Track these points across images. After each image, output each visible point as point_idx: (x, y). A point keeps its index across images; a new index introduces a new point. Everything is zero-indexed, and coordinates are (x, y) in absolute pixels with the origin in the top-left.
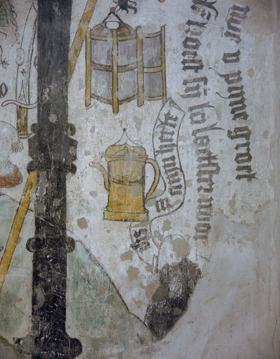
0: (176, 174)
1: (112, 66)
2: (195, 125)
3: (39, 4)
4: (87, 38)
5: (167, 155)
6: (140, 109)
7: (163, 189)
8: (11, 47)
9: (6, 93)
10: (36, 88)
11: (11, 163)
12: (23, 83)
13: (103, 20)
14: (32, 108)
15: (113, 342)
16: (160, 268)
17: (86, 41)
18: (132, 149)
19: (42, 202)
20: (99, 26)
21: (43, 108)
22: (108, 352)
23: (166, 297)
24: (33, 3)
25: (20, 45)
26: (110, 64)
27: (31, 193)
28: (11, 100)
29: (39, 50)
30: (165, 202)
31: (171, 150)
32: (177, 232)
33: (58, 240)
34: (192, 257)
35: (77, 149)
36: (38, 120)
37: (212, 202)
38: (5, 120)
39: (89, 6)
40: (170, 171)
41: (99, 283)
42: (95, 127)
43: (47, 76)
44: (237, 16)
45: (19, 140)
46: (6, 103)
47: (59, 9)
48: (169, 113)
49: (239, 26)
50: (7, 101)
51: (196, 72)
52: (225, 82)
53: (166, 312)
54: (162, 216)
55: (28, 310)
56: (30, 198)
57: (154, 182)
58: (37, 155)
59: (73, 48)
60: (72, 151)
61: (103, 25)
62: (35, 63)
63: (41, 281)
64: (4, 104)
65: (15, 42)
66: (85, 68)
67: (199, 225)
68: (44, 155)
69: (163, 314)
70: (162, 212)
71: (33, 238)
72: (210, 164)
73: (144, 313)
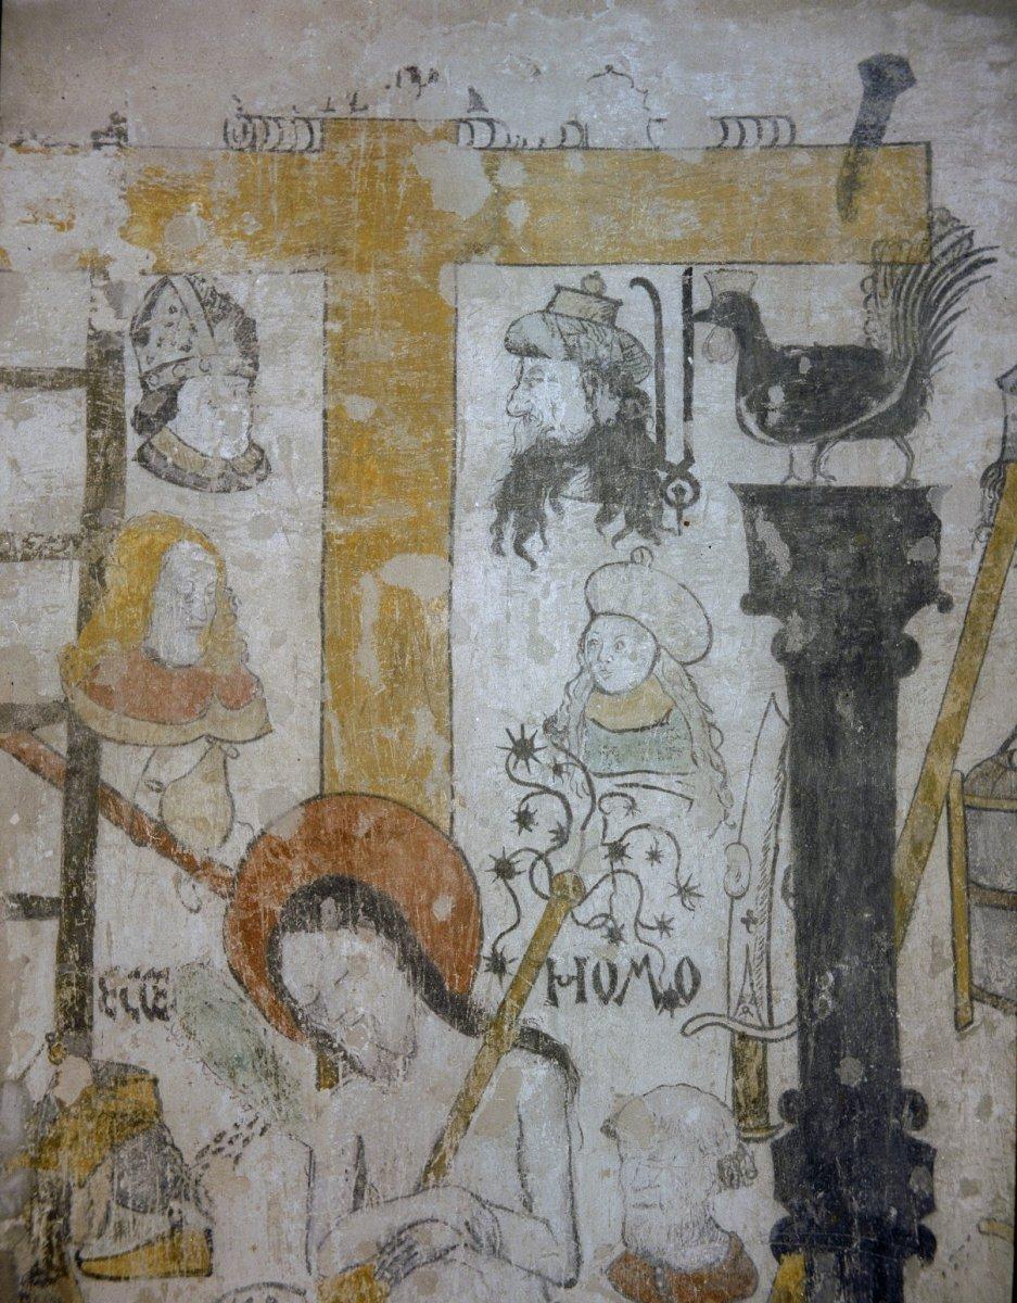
3: (792, 698)
4: (952, 805)
8: (705, 839)
9: (694, 992)
10: (791, 972)
11: (717, 1226)
13: (1000, 743)
14: (782, 1039)
17: (949, 814)
20: (990, 763)
21: (817, 1039)
24: (773, 694)
25: (736, 832)
28: (713, 1015)
29: (796, 844)
35: (937, 1175)
36: (803, 1078)
39: (955, 700)
42: (989, 1097)
43: (827, 932)
45: (740, 1146)
47: (857, 710)
50: (698, 1017)
58: (804, 1196)
59: (907, 838)
60: (918, 1183)
61: (1003, 759)
62: (784, 889)
64: (691, 1027)
66: (948, 903)
68: (825, 1197)
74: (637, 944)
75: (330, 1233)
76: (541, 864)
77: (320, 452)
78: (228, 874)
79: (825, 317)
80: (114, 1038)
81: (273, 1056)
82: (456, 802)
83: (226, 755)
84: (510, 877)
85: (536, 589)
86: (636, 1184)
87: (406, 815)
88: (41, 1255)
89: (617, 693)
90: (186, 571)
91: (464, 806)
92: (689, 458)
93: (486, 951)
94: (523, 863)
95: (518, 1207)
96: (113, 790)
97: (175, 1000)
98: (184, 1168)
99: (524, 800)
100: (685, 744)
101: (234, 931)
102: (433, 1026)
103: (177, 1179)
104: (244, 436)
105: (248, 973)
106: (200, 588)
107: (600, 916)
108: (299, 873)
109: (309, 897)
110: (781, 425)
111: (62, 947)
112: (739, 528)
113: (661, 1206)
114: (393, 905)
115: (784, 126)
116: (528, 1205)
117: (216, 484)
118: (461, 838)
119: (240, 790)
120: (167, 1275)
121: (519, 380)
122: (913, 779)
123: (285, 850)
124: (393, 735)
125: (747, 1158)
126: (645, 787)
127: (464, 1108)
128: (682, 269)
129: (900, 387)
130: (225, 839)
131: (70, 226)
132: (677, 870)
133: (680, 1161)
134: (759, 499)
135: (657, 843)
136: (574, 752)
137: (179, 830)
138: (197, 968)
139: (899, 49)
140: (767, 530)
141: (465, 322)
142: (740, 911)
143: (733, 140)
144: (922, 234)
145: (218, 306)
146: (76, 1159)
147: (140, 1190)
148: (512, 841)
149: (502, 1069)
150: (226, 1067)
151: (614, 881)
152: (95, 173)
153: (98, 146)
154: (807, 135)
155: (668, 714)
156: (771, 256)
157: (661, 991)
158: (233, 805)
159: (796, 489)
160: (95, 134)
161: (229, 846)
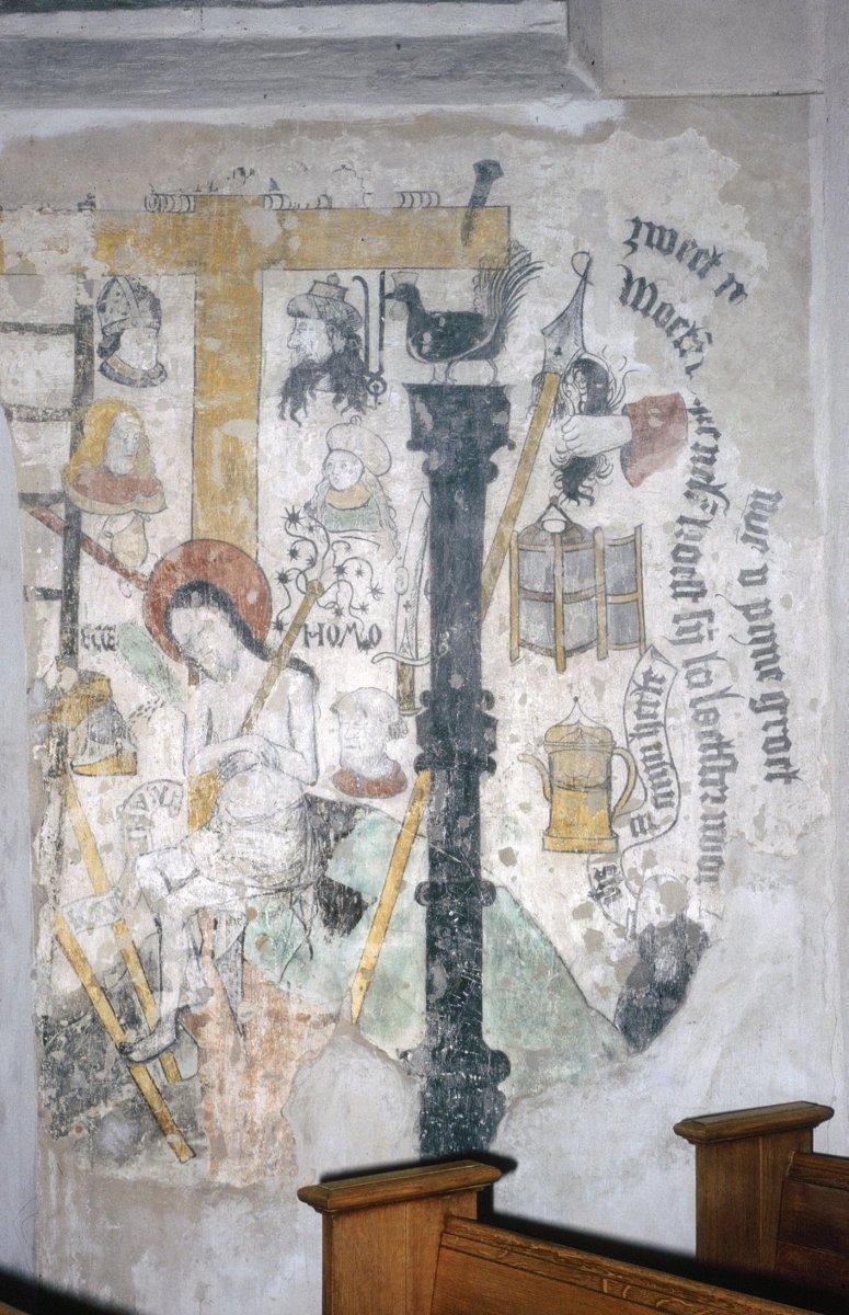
0: (664, 773)
1: (554, 593)
2: (695, 690)
3: (432, 493)
5: (648, 741)
6: (601, 665)
7: (642, 797)
9: (378, 641)
15: (563, 1056)
16: (638, 931)
18: (589, 731)
21: (440, 665)
22: (553, 1073)
23: (651, 980)
26: (551, 590)
30: (645, 820)
31: (655, 733)
32: (667, 871)
33: (468, 885)
34: (692, 913)
35: (498, 732)
37: (725, 820)
38: (377, 686)
40: (653, 767)
41: (537, 957)
44: (762, 508)
46: (380, 657)
48: (650, 672)
49: (764, 525)
51: (695, 601)
52: (745, 619)
53: (649, 1005)
54: (642, 843)
55: (419, 1001)
57: (627, 787)
61: (539, 525)
62: (425, 591)
64: (376, 659)
66: (508, 597)
67: (704, 858)
69: (646, 1009)
70: (642, 837)
71: (426, 883)
72: (720, 756)
73: (613, 1007)
77: (192, 367)
79: (453, 297)
80: (89, 659)
85: (301, 437)
88: (54, 762)
89: (342, 491)
90: (124, 428)
92: (381, 369)
93: (274, 619)
94: (293, 575)
95: (288, 746)
104: (154, 359)
105: (155, 628)
106: (131, 436)
108: (181, 579)
110: (430, 353)
111: (63, 614)
112: (406, 406)
114: (227, 595)
115: (434, 197)
116: (293, 744)
117: (139, 383)
118: (261, 563)
120: (115, 774)
121: (294, 329)
122: (492, 535)
123: (173, 567)
127: (261, 696)
128: (380, 271)
129: (491, 334)
130: (143, 562)
131: (67, 252)
133: (370, 726)
134: (418, 392)
137: (120, 557)
139: (494, 157)
140: (421, 407)
141: (266, 300)
142: (403, 600)
143: (406, 205)
144: (505, 254)
145: (141, 292)
148: (287, 564)
149: (281, 678)
150: (143, 674)
152: (79, 224)
153: (81, 210)
154: (446, 201)
156: (428, 264)
159: (436, 386)
160: (79, 204)
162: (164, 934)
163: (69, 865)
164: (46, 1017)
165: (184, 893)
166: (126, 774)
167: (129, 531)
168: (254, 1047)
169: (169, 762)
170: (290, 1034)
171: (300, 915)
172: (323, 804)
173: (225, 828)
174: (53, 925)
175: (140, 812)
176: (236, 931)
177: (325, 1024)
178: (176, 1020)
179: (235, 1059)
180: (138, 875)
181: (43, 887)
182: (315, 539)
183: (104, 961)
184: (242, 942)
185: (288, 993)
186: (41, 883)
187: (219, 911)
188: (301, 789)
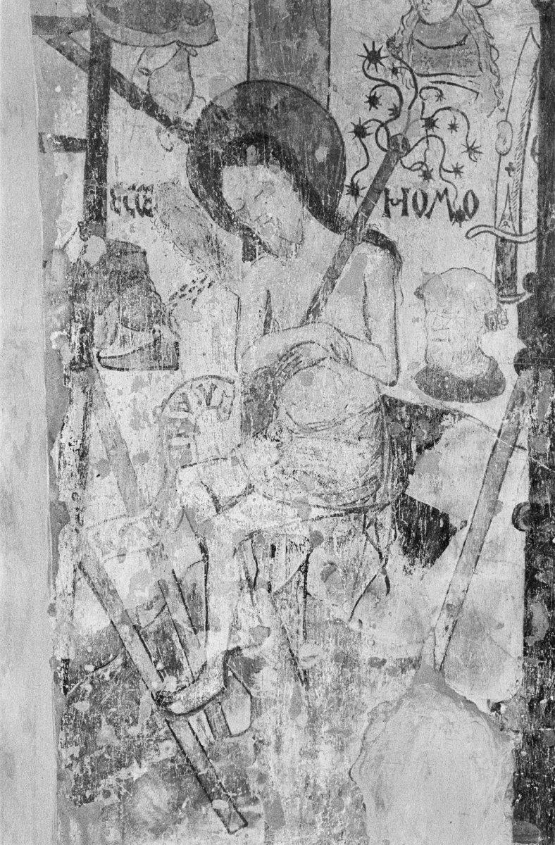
3: (543, 31)
8: (486, 118)
9: (474, 212)
11: (483, 353)
12: (508, 192)
14: (527, 242)
19: (542, 432)
24: (531, 28)
27: (521, 413)
28: (486, 226)
36: (538, 267)
45: (498, 306)
46: (476, 231)
55: (516, 645)
56: (519, 424)
58: (535, 336)
62: (533, 150)
63: (540, 590)
64: (472, 233)
65: (495, 108)
68: (547, 336)
74: (441, 181)
75: (249, 347)
76: (382, 129)
78: (190, 128)
80: (120, 226)
81: (216, 241)
82: (332, 87)
83: (189, 54)
84: (364, 137)
86: (435, 327)
87: (300, 96)
88: (76, 353)
89: (434, 24)
91: (336, 91)
93: (347, 182)
94: (372, 128)
95: (363, 337)
96: (119, 74)
97: (157, 205)
98: (162, 306)
99: (373, 89)
100: (475, 57)
101: (193, 164)
102: (314, 226)
103: (158, 311)
105: (202, 189)
107: (419, 163)
109: (240, 144)
111: (88, 170)
113: (449, 341)
116: (368, 336)
118: (333, 111)
119: (197, 76)
120: (152, 368)
123: (225, 115)
124: (292, 45)
125: (503, 313)
126: (449, 83)
127: (332, 275)
130: (188, 107)
132: (467, 136)
135: (455, 119)
136: (405, 60)
137: (159, 100)
138: (170, 186)
142: (505, 163)
146: (97, 297)
147: (135, 318)
148: (366, 115)
151: (428, 141)
155: (465, 38)
157: (454, 210)
158: (193, 86)
161: (190, 111)
162: (210, 562)
163: (96, 479)
164: (66, 661)
165: (235, 513)
166: (165, 368)
167: (170, 68)
168: (318, 696)
169: (218, 356)
170: (361, 683)
171: (375, 542)
172: (404, 409)
173: (285, 435)
174: (76, 550)
175: (183, 415)
176: (298, 560)
177: (403, 670)
178: (224, 664)
179: (295, 711)
180: (180, 491)
181: (64, 505)
182: (399, 84)
183: (138, 594)
184: (306, 571)
185: (360, 633)
186: (61, 499)
187: (277, 535)
188: (378, 389)
